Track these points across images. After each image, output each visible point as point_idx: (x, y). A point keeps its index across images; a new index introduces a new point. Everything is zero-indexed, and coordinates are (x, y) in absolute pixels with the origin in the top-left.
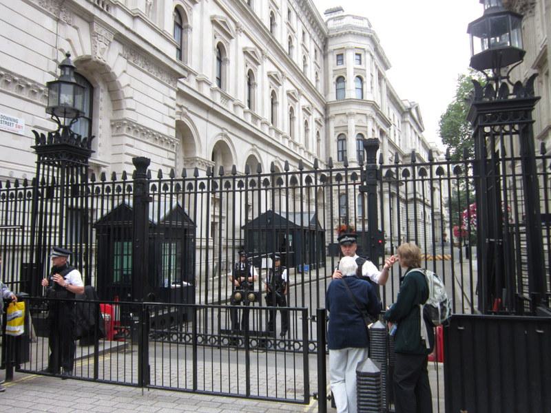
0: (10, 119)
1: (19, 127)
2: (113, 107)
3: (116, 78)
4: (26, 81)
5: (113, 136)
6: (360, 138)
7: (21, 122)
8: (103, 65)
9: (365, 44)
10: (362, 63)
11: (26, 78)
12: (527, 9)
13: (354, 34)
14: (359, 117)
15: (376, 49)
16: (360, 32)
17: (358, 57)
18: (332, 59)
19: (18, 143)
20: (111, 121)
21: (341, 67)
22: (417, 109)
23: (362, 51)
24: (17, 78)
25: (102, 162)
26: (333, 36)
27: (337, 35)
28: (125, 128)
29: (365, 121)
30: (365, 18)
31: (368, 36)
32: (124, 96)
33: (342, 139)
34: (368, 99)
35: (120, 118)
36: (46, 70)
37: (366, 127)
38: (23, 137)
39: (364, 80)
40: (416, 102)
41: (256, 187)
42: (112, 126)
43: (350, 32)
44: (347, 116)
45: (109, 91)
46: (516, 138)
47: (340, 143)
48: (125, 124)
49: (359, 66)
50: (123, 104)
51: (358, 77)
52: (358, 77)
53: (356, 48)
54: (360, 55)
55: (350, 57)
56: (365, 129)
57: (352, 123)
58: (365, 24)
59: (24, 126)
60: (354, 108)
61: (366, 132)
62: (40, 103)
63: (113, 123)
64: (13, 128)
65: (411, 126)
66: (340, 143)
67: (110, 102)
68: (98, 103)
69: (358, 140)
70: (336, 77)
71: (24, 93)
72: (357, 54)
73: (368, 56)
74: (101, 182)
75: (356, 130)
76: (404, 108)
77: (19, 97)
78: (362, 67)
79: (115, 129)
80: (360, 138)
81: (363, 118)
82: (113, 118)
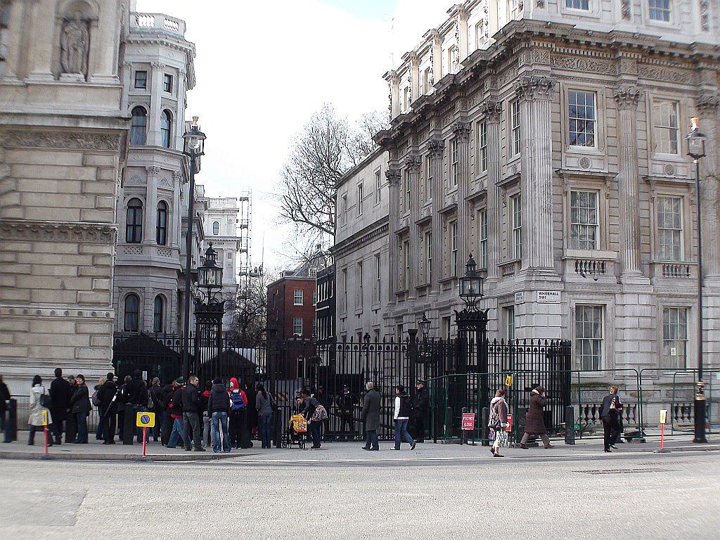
10: (174, 88)
13: (167, 45)
14: (162, 174)
17: (166, 80)
18: (129, 80)
21: (141, 92)
23: (174, 71)
26: (136, 42)
27: (143, 42)
29: (170, 181)
33: (136, 207)
43: (162, 43)
44: (147, 172)
46: (475, 332)
47: (132, 211)
49: (167, 95)
51: (165, 111)
52: (165, 111)
54: (170, 77)
55: (158, 80)
57: (154, 183)
60: (159, 161)
66: (132, 211)
69: (159, 210)
70: (132, 107)
81: (169, 176)
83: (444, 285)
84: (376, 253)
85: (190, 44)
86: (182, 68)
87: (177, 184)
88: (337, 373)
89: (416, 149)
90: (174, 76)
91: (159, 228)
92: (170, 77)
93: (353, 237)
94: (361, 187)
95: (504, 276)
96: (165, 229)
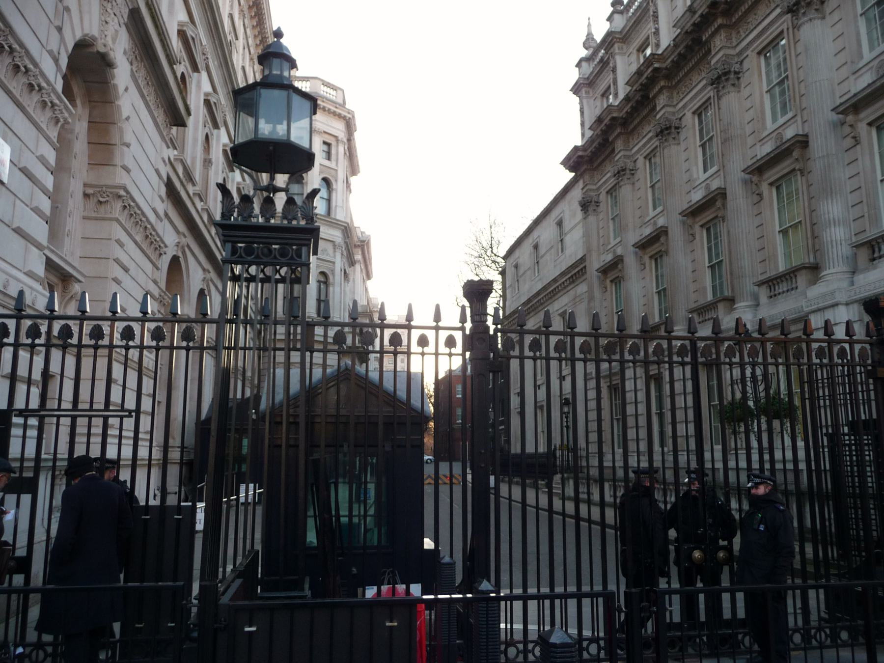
2: (90, 157)
3: (117, 97)
5: (84, 218)
6: (322, 279)
9: (338, 128)
10: (333, 157)
12: (669, 134)
15: (349, 140)
16: (333, 109)
17: (325, 148)
20: (85, 185)
22: (368, 243)
25: (78, 271)
28: (119, 205)
30: (340, 89)
31: (344, 118)
32: (121, 137)
34: (338, 218)
35: (109, 183)
37: (334, 263)
39: (334, 187)
40: (367, 233)
41: (592, 356)
42: (86, 196)
48: (120, 197)
49: (327, 163)
50: (117, 152)
53: (325, 132)
54: (328, 145)
56: (330, 265)
58: (340, 101)
61: (333, 272)
63: (90, 191)
65: (361, 271)
67: (86, 145)
69: (319, 282)
72: (325, 143)
73: (341, 149)
74: (435, 324)
75: (318, 266)
76: (356, 239)
78: (332, 164)
79: (93, 201)
80: (322, 279)
82: (92, 180)
83: (699, 314)
84: (560, 311)
85: (349, 112)
86: (342, 136)
87: (338, 255)
88: (513, 451)
89: (628, 153)
90: (334, 143)
91: (319, 301)
92: (328, 145)
93: (529, 300)
94: (536, 247)
95: (874, 259)
96: (327, 302)
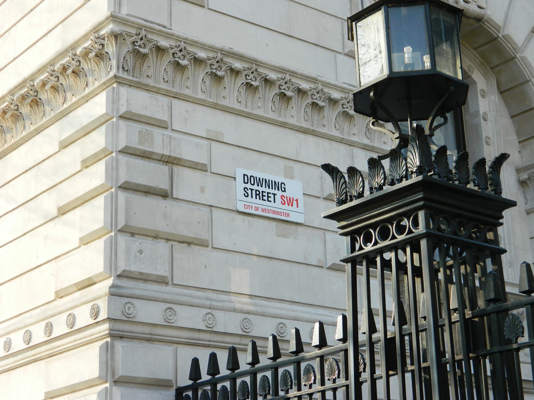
0: (268, 184)
1: (290, 202)
2: (518, 133)
4: (294, 80)
7: (294, 189)
8: (479, 19)
11: (293, 74)
19: (290, 246)
24: (272, 76)
36: (341, 51)
38: (300, 229)
45: (501, 93)
59: (301, 200)
62: (336, 133)
64: (277, 206)
67: (506, 121)
68: (477, 128)
71: (293, 112)
77: (283, 125)
